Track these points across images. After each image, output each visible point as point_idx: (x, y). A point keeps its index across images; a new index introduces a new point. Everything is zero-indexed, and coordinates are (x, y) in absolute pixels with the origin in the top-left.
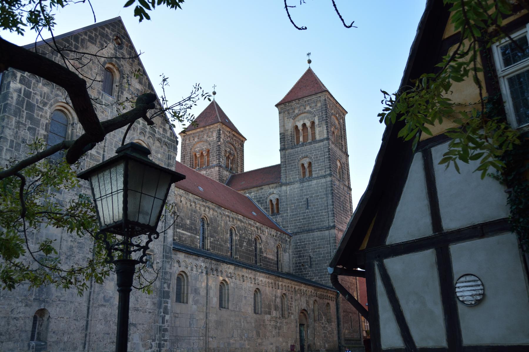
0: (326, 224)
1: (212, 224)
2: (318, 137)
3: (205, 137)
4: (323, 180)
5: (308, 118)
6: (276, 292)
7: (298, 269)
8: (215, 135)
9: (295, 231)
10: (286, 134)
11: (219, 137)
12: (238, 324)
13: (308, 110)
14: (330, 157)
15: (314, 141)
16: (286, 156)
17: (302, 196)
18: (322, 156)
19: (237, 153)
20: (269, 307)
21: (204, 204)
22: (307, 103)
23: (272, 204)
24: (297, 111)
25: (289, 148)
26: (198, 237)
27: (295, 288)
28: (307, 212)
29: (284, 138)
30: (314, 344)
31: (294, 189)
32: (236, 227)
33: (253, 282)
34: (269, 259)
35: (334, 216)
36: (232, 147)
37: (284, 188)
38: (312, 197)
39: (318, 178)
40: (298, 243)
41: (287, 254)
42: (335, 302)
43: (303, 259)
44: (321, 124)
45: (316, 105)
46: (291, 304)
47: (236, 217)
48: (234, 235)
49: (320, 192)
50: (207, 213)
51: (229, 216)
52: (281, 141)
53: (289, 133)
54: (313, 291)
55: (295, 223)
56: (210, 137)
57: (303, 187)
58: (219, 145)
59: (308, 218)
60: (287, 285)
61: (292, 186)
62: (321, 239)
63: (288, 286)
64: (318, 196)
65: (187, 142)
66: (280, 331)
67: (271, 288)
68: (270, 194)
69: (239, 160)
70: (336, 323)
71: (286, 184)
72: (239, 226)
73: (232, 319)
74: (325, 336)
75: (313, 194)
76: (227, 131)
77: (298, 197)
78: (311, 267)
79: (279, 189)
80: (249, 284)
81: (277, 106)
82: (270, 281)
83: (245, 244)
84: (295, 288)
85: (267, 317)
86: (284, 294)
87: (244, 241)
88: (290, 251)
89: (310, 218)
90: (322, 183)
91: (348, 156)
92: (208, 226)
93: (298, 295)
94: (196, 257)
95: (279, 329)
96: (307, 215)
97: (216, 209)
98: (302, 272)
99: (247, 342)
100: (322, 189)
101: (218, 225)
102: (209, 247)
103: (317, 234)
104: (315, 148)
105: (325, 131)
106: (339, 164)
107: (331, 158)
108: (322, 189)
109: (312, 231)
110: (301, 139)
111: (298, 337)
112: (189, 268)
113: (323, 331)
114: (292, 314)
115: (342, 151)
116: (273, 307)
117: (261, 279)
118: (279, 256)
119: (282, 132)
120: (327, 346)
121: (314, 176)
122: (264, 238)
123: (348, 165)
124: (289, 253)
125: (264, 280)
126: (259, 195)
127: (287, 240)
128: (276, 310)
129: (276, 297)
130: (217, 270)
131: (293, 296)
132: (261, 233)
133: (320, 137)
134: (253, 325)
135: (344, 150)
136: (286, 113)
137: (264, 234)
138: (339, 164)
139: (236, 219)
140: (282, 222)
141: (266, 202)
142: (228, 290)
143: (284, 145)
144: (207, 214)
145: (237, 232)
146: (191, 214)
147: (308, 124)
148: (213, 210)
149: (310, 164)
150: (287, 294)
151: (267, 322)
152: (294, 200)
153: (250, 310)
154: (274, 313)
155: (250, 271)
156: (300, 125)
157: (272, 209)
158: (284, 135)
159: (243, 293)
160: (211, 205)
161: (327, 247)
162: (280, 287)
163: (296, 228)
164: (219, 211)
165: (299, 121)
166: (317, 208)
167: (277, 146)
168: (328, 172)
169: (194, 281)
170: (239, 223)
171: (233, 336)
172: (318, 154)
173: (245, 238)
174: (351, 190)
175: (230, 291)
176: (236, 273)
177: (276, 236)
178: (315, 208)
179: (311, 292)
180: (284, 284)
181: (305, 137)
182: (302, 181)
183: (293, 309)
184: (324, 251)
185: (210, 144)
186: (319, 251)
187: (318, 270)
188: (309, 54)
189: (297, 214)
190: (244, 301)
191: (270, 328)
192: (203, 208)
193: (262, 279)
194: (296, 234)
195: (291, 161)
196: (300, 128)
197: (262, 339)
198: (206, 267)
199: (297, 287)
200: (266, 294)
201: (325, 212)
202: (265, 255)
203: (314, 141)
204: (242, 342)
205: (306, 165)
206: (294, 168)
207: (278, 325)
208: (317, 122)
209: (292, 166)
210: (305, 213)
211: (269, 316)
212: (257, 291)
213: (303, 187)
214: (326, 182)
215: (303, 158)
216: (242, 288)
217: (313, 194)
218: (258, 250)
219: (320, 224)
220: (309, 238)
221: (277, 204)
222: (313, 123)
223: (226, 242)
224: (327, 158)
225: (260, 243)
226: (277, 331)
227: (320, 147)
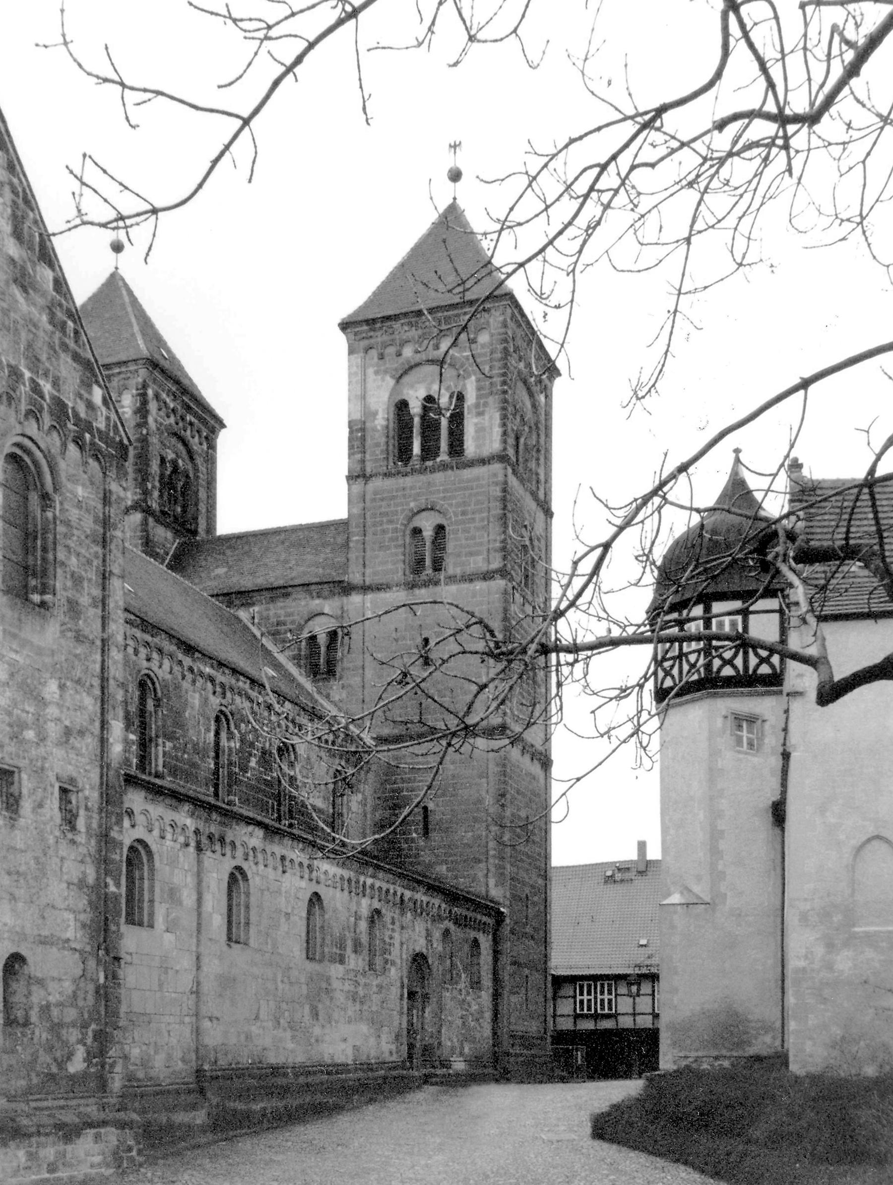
6: (358, 904)
16: (368, 497)
21: (148, 638)
33: (306, 876)
50: (154, 665)
52: (351, 447)
63: (388, 891)
67: (346, 892)
82: (346, 874)
83: (253, 763)
92: (157, 706)
93: (409, 914)
94: (174, 802)
97: (180, 656)
102: (160, 768)
112: (156, 833)
116: (349, 944)
119: (357, 416)
128: (355, 952)
129: (358, 918)
130: (222, 840)
142: (248, 894)
143: (363, 461)
144: (155, 669)
150: (383, 911)
153: (297, 950)
164: (187, 661)
169: (167, 868)
171: (257, 1018)
180: (378, 884)
183: (395, 952)
190: (284, 927)
192: (143, 652)
198: (197, 832)
199: (408, 894)
200: (335, 910)
204: (279, 1033)
207: (361, 993)
212: (316, 899)
216: (279, 892)
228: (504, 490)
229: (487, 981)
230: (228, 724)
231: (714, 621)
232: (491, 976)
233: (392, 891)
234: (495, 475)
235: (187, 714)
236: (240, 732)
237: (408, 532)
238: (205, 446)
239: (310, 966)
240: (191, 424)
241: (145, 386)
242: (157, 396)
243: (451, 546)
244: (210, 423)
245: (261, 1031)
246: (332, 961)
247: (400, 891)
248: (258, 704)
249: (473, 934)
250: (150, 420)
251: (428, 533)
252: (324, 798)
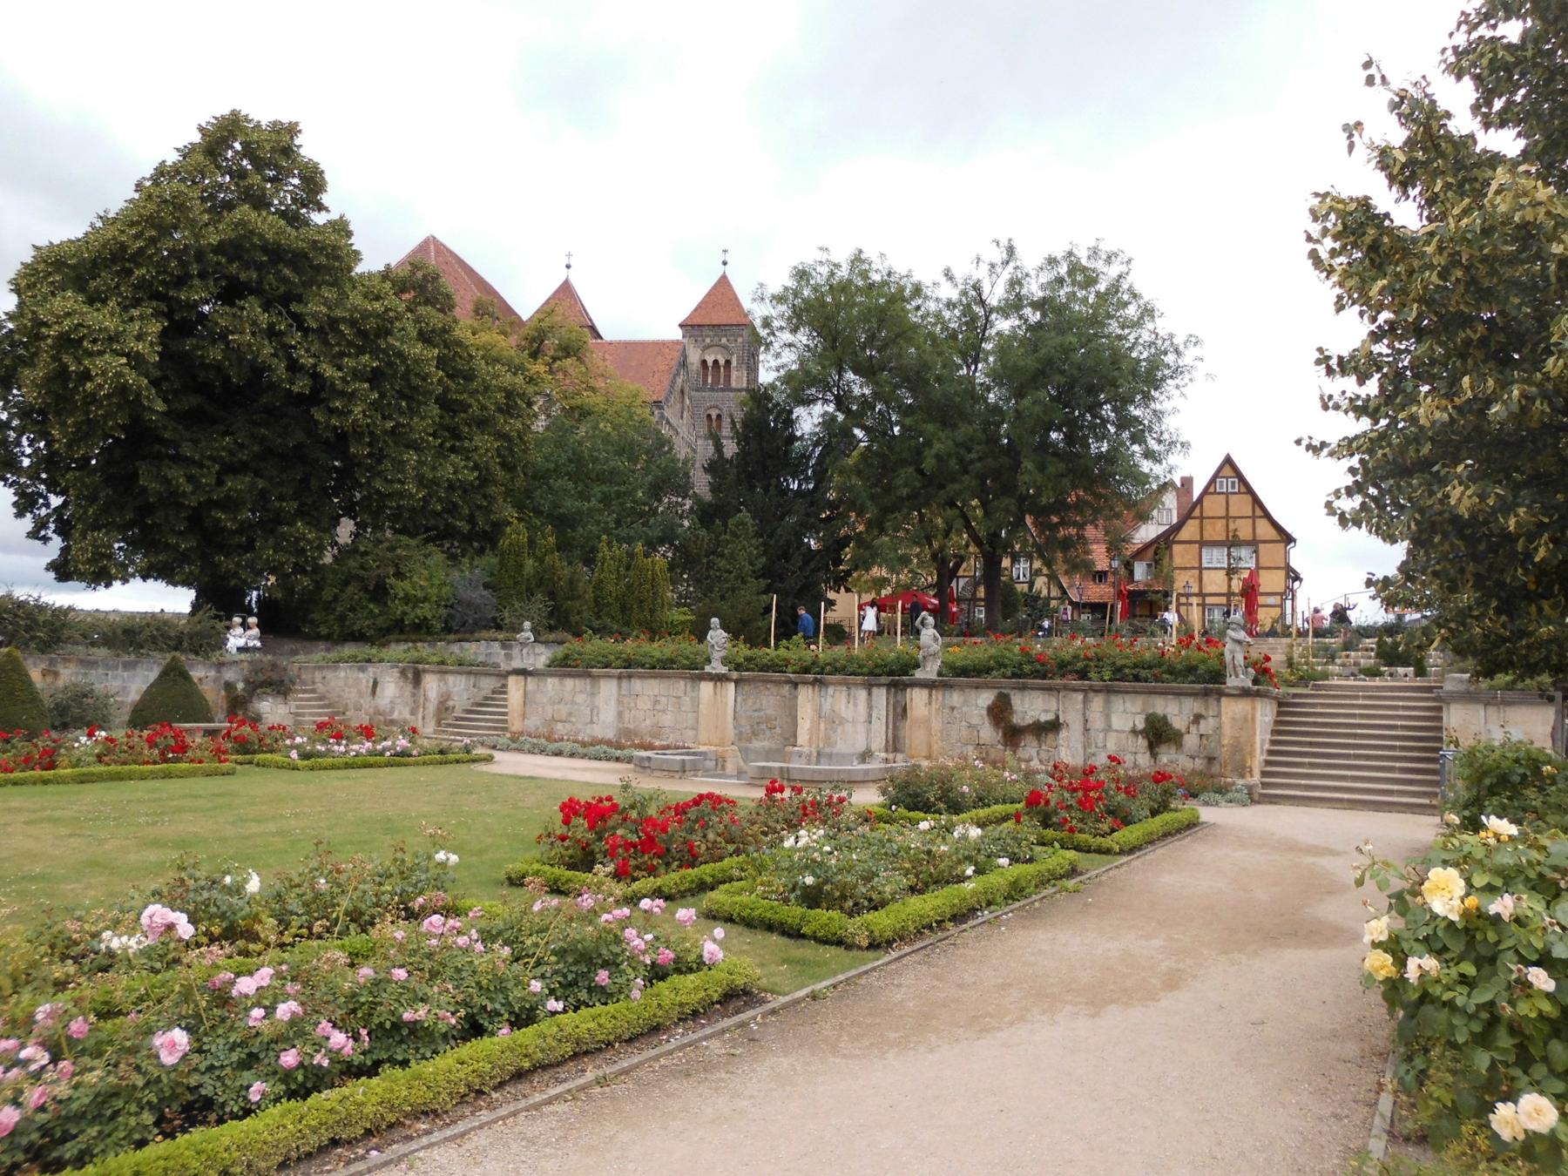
2: (734, 384)
15: (728, 388)
24: (708, 340)
81: (681, 326)
147: (722, 362)
149: (719, 416)
156: (710, 360)
181: (716, 380)
196: (710, 363)
203: (728, 388)
208: (734, 363)
222: (728, 362)
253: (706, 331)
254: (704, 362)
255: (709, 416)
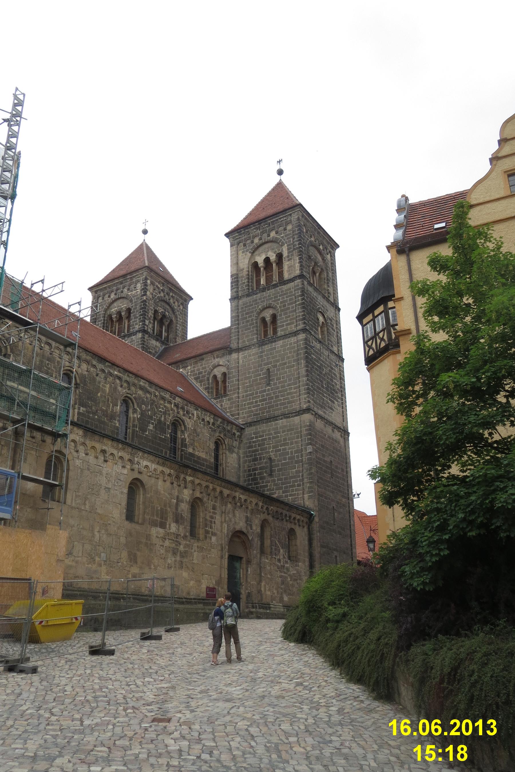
0: (296, 407)
1: (85, 384)
2: (286, 276)
3: (125, 290)
4: (293, 339)
5: (273, 249)
7: (253, 480)
8: (139, 286)
9: (249, 420)
10: (240, 275)
11: (145, 290)
12: (85, 533)
13: (273, 237)
14: (303, 303)
15: (282, 282)
16: (240, 307)
17: (261, 365)
18: (292, 303)
19: (176, 317)
20: (163, 514)
22: (271, 226)
23: (217, 382)
25: (243, 296)
26: (52, 401)
27: (221, 492)
28: (269, 390)
29: (238, 281)
30: (259, 591)
31: (250, 356)
32: (135, 398)
33: (128, 467)
34: (199, 458)
35: (308, 393)
36: (168, 307)
37: (234, 356)
38: (275, 366)
39: (285, 336)
40: (253, 438)
41: (235, 455)
42: (306, 529)
43: (259, 464)
44: (292, 255)
45: (285, 229)
46: (212, 517)
47: (136, 382)
48: (131, 411)
49: (288, 358)
51: (120, 378)
52: (232, 286)
53: (245, 273)
54: (260, 504)
55: (249, 408)
56: (132, 291)
57: (262, 352)
58: (145, 301)
59: (269, 399)
60: (204, 484)
61: (246, 352)
62: (288, 431)
63: (207, 487)
64: (285, 364)
65: (100, 300)
66: (185, 560)
67: (168, 483)
68: (215, 367)
69: (179, 328)
70: (307, 564)
71: (238, 350)
72: (140, 397)
73: (72, 522)
74: (283, 583)
75: (278, 361)
76: (159, 283)
77: (254, 367)
78: (271, 475)
79: (228, 357)
80: (118, 468)
81: (227, 235)
82: (167, 471)
83: (151, 427)
84: (221, 492)
85: (156, 532)
86: (198, 498)
87: (149, 423)
88: (241, 451)
89: (272, 398)
90: (291, 344)
91: (339, 310)
92: (76, 388)
95: (182, 556)
96: (267, 395)
97: (94, 363)
98: (258, 483)
99: (104, 568)
100: (290, 353)
101: (98, 390)
103: (281, 422)
104: (283, 291)
105: (297, 265)
106: (321, 319)
107: (310, 310)
108: (290, 353)
109: (275, 418)
110: (263, 281)
111: (225, 574)
113: (279, 574)
114: (214, 534)
115: (328, 301)
117: (145, 463)
118: (220, 457)
120: (286, 599)
121: (279, 333)
122: (189, 423)
123: (338, 323)
124: (238, 454)
125: (153, 466)
126: (198, 370)
127: (234, 434)
128: (177, 522)
129: (179, 500)
131: (218, 505)
132: (184, 415)
133: (289, 274)
134: (123, 540)
135: (331, 299)
136: (242, 244)
137: (190, 418)
138: (321, 319)
139: (134, 385)
140: (230, 408)
141: (208, 380)
143: (238, 292)
145: (136, 407)
146: (41, 362)
147: (273, 257)
148: (88, 362)
150: (205, 499)
151: (155, 540)
152: (249, 373)
153: (117, 513)
154: (173, 528)
155: (120, 446)
157: (217, 389)
158: (237, 278)
159: (103, 481)
160: (84, 356)
161: (296, 442)
162: (189, 485)
163: (250, 416)
164: (100, 366)
165: (259, 255)
166: (283, 382)
167: (227, 292)
168: (301, 326)
170: (140, 392)
172: (286, 301)
173: (151, 417)
174: (343, 360)
175: (71, 473)
176: (88, 442)
177: (213, 424)
178: (279, 383)
179: (256, 504)
180: (197, 481)
181: (269, 279)
182: (261, 343)
184: (292, 448)
185: (131, 301)
186: (285, 449)
187: (281, 479)
188: (279, 162)
189: (253, 394)
191: (162, 551)
193: (146, 464)
194: (250, 424)
195: (246, 314)
197: (141, 568)
199: (226, 492)
200: (157, 492)
201: (294, 389)
202: (190, 450)
204: (94, 567)
205: (268, 319)
206: (250, 325)
208: (285, 254)
209: (248, 321)
210: (265, 391)
211: (161, 531)
213: (262, 352)
214: (298, 341)
215: (264, 309)
216: (101, 473)
217: (278, 361)
218: (179, 441)
219: (287, 407)
220: (269, 430)
221: (224, 381)
222: (280, 256)
223: (112, 417)
224: (299, 305)
225: (183, 432)
226: (178, 558)
227: (290, 289)
228: (303, 291)
229: (304, 556)
230: (133, 403)
231: (390, 311)
232: (307, 554)
233: (211, 488)
234: (298, 285)
235: (99, 394)
236: (141, 409)
237: (259, 321)
238: (181, 307)
239: (127, 523)
240: (172, 296)
241: (146, 279)
242: (152, 283)
243: (279, 323)
244: (185, 298)
245: (74, 564)
246: (154, 524)
247: (218, 489)
248: (156, 396)
249: (289, 526)
250: (148, 293)
251: (268, 319)
252: (207, 453)
253: (253, 231)
254: (255, 265)
255: (263, 320)
